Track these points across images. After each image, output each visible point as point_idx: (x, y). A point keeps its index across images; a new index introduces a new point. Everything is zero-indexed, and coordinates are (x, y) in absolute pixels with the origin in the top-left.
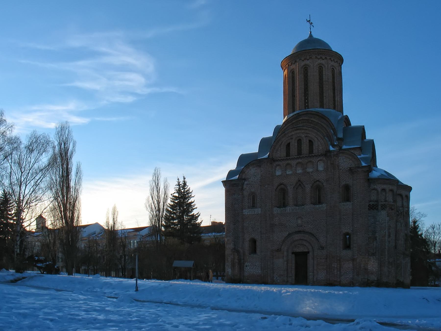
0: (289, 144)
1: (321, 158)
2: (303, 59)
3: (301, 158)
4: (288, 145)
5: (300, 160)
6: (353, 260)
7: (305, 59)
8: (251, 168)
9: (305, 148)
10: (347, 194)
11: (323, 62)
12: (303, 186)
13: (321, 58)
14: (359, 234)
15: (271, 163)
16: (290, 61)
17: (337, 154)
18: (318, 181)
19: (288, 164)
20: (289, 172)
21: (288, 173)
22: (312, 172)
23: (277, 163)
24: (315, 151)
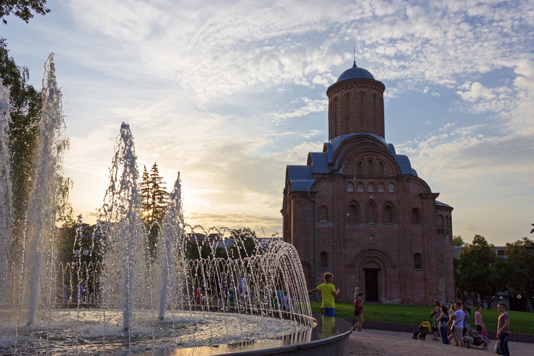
0: (361, 163)
5: (372, 180)
6: (425, 280)
7: (362, 86)
8: (323, 181)
11: (376, 92)
12: (374, 205)
15: (344, 180)
18: (390, 202)
21: (359, 191)
22: (383, 193)
23: (349, 180)
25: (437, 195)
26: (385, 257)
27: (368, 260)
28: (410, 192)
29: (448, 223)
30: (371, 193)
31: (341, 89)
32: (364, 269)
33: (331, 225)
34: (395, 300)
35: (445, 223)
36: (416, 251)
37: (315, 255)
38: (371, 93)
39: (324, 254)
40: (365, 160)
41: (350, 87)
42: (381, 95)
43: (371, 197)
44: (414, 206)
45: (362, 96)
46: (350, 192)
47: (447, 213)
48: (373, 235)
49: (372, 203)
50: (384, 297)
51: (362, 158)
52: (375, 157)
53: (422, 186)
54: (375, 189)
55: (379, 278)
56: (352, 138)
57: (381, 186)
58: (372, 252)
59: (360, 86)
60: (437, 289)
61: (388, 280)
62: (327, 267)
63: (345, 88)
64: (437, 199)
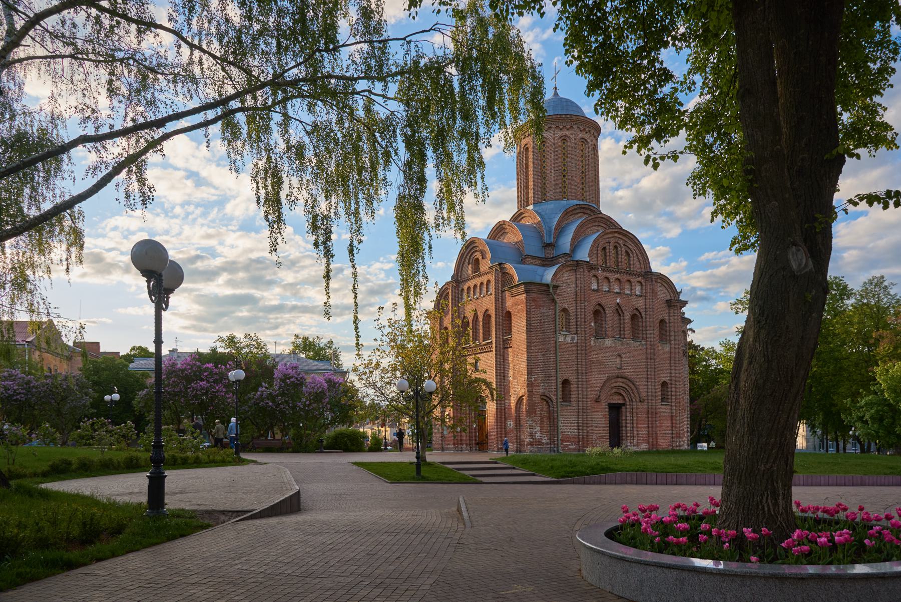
0: (604, 248)
1: (639, 279)
5: (618, 276)
23: (593, 272)
26: (633, 387)
27: (613, 391)
31: (553, 127)
36: (663, 379)
39: (566, 382)
41: (568, 127)
44: (660, 318)
46: (594, 290)
48: (619, 356)
49: (619, 310)
52: (621, 242)
54: (621, 289)
57: (627, 286)
58: (620, 380)
59: (582, 128)
62: (570, 402)
63: (561, 127)
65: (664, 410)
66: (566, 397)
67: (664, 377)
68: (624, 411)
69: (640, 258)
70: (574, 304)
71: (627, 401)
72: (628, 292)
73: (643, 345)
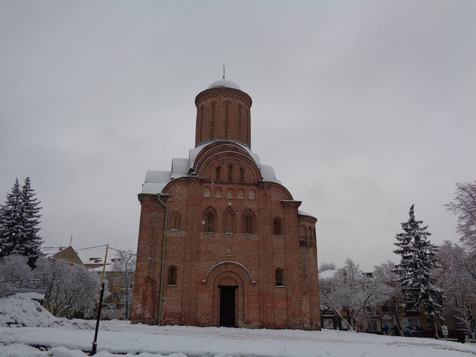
0: (220, 167)
1: (253, 187)
2: (225, 95)
3: (233, 184)
4: (219, 169)
5: (231, 186)
6: (287, 299)
8: (176, 184)
9: (236, 174)
10: (277, 226)
11: (242, 103)
13: (241, 99)
14: (292, 270)
15: (201, 184)
16: (199, 99)
17: (269, 186)
18: (250, 210)
19: (218, 188)
20: (218, 196)
21: (217, 196)
22: (243, 200)
23: (206, 184)
24: (246, 180)
25: (299, 203)
28: (272, 200)
29: (311, 235)
30: (230, 199)
32: (219, 287)
33: (184, 234)
34: (254, 323)
35: (309, 235)
37: (161, 269)
38: (236, 103)
40: (225, 164)
42: (247, 107)
43: (230, 204)
45: (227, 105)
46: (206, 198)
47: (311, 225)
49: (230, 211)
50: (241, 320)
51: (221, 162)
53: (284, 194)
54: (234, 196)
55: (236, 297)
56: (215, 144)
60: (301, 310)
61: (246, 299)
63: (211, 96)
64: (300, 209)
65: (280, 291)
66: (172, 281)
67: (279, 264)
68: (236, 292)
69: (254, 172)
70: (185, 208)
71: (240, 284)
72: (242, 198)
73: (255, 237)
